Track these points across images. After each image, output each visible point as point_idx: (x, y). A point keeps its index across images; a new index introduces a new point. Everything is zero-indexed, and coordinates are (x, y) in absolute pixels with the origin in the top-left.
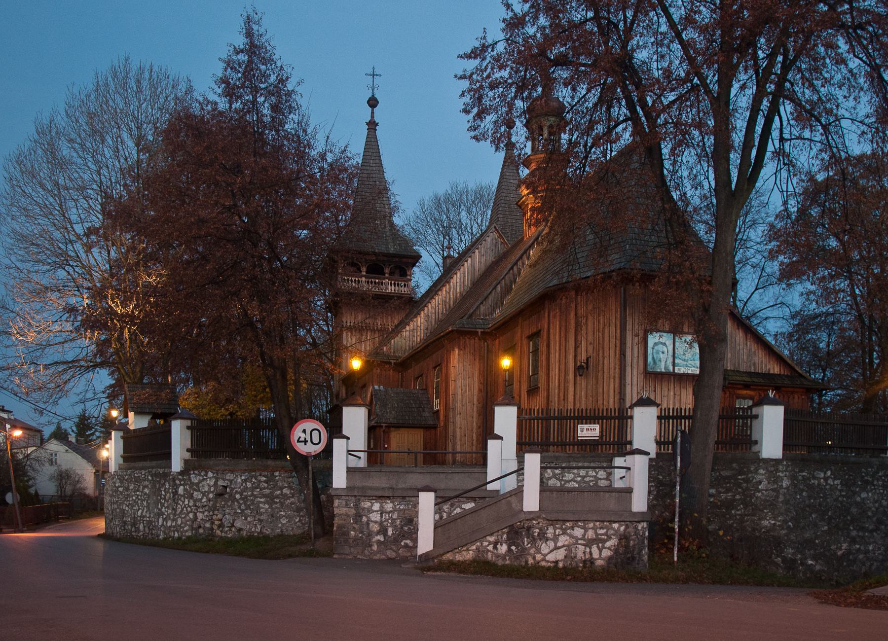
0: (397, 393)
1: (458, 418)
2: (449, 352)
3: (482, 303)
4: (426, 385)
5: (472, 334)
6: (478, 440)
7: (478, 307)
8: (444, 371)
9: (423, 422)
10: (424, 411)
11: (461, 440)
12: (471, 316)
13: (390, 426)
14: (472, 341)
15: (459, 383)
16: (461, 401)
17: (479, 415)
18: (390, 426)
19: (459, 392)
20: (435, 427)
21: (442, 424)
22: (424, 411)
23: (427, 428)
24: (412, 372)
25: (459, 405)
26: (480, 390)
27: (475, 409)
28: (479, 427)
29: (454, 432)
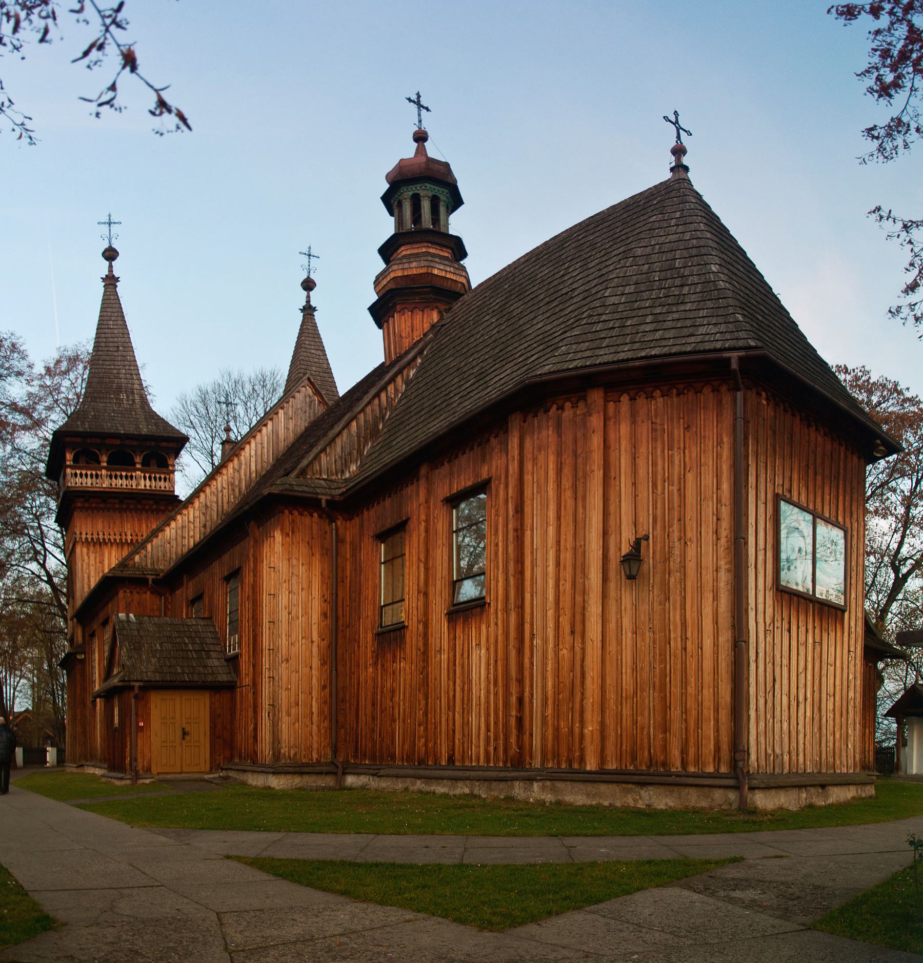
1: (283, 670)
2: (258, 544)
3: (324, 450)
4: (211, 611)
5: (305, 503)
6: (321, 712)
7: (317, 457)
8: (248, 578)
11: (289, 715)
12: (303, 472)
13: (150, 687)
14: (307, 520)
15: (283, 600)
16: (289, 636)
17: (323, 663)
18: (150, 687)
19: (284, 616)
20: (230, 687)
21: (247, 681)
22: (209, 657)
24: (188, 590)
25: (283, 642)
26: (324, 615)
27: (315, 650)
28: (324, 687)
29: (274, 698)
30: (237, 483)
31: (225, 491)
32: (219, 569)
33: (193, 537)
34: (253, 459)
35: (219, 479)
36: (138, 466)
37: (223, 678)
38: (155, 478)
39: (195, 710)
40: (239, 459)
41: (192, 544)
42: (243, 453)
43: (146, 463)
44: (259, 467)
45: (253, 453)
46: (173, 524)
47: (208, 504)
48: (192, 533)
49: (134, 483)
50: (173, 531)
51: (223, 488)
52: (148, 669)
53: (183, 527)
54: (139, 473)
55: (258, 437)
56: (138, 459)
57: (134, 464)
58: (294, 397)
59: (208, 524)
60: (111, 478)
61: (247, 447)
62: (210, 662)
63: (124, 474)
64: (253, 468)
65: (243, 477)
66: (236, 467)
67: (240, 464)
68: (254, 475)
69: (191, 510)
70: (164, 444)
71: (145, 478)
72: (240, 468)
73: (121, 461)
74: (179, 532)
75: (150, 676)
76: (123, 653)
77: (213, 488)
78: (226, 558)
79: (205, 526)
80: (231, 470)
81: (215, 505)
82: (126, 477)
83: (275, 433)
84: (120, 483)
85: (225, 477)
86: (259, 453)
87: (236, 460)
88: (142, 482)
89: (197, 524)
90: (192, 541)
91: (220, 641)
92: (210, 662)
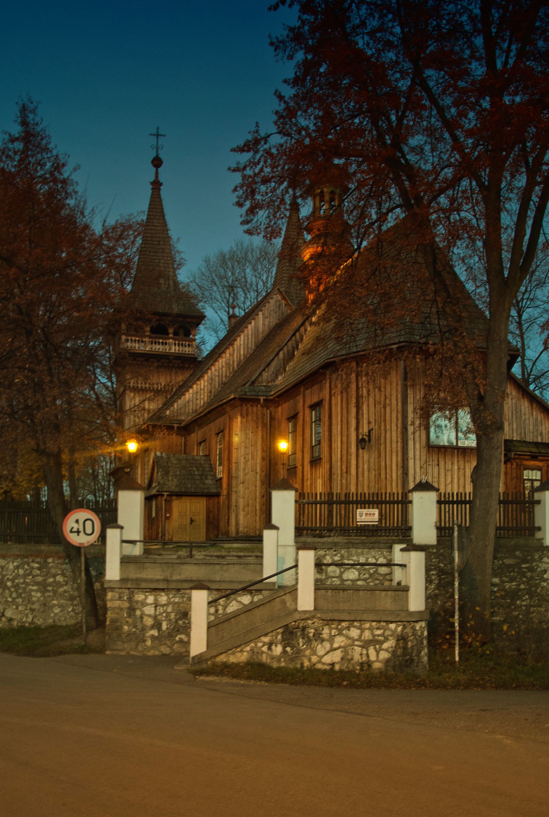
0: (179, 460)
9: (206, 491)
10: (206, 479)
13: (172, 494)
22: (206, 479)
23: (210, 496)
30: (231, 363)
31: (224, 369)
32: (213, 427)
33: (203, 398)
34: (242, 347)
35: (220, 361)
36: (171, 335)
37: (214, 490)
38: (182, 345)
39: (197, 507)
40: (233, 347)
41: (202, 403)
42: (236, 343)
43: (176, 334)
44: (246, 352)
45: (242, 343)
46: (191, 391)
47: (213, 377)
48: (202, 397)
49: (167, 347)
50: (191, 395)
51: (223, 367)
52: (172, 484)
53: (197, 392)
54: (171, 340)
55: (246, 331)
56: (171, 331)
57: (168, 334)
58: (269, 302)
59: (213, 390)
60: (152, 343)
61: (239, 339)
62: (207, 482)
63: (161, 341)
64: (242, 352)
65: (235, 359)
66: (231, 353)
67: (234, 350)
68: (242, 357)
69: (202, 381)
70: (189, 320)
71: (175, 344)
72: (234, 353)
73: (160, 331)
74: (195, 395)
75: (173, 489)
76: (158, 476)
77: (217, 367)
78: (217, 421)
79: (211, 392)
80: (228, 355)
81: (217, 378)
82: (162, 343)
83: (256, 328)
84: (159, 348)
85: (224, 360)
86: (246, 342)
87: (231, 349)
88: (172, 347)
89: (206, 391)
90: (202, 401)
91: (212, 469)
92: (207, 482)
